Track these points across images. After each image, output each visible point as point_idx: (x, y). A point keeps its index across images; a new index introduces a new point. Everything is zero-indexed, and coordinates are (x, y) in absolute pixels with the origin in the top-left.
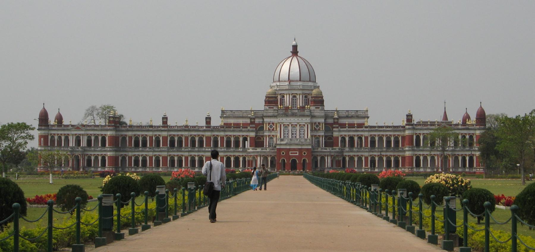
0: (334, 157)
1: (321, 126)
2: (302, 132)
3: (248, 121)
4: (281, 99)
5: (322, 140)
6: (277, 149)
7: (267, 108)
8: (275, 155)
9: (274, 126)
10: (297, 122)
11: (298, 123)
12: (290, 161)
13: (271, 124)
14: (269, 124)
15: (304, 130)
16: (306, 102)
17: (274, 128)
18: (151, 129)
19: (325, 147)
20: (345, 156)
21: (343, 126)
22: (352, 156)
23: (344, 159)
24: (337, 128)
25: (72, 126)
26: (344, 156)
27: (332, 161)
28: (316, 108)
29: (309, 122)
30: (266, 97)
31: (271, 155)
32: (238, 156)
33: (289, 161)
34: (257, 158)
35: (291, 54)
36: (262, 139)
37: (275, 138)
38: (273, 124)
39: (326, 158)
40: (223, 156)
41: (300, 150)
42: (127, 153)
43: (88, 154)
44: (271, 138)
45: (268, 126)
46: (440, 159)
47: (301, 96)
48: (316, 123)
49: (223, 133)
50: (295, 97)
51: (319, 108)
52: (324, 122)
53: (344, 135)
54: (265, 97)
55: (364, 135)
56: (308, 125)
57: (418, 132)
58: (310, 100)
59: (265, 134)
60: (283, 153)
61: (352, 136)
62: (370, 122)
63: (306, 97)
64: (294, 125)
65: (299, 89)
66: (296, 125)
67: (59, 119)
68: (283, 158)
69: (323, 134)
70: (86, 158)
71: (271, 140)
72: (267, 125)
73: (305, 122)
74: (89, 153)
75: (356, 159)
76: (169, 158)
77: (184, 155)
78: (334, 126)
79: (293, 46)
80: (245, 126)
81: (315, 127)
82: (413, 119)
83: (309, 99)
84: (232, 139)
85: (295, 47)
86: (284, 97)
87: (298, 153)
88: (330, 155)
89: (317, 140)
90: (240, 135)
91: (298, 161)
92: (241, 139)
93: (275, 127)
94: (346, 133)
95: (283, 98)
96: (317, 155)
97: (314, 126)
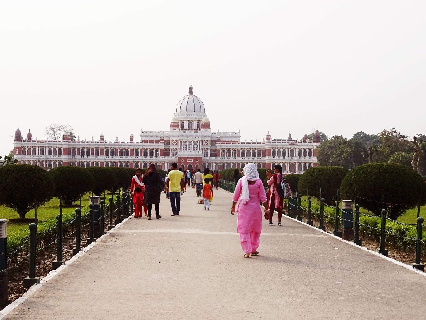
0: (217, 164)
1: (208, 143)
2: (196, 146)
3: (159, 139)
4: (181, 124)
5: (209, 152)
6: (179, 157)
7: (171, 129)
8: (177, 162)
14: (173, 140)
15: (196, 145)
16: (199, 126)
17: (176, 143)
18: (93, 143)
19: (211, 156)
20: (225, 163)
21: (223, 142)
22: (229, 163)
23: (224, 164)
24: (219, 143)
25: (38, 141)
26: (224, 163)
27: (216, 166)
28: (205, 130)
29: (201, 139)
30: (171, 123)
34: (165, 164)
35: (188, 94)
36: (168, 151)
37: (177, 150)
38: (176, 140)
39: (212, 164)
41: (195, 159)
42: (76, 160)
43: (49, 161)
44: (175, 150)
46: (289, 165)
47: (195, 122)
48: (205, 140)
50: (191, 122)
52: (210, 140)
56: (199, 142)
57: (274, 147)
58: (201, 125)
59: (170, 148)
60: (183, 161)
62: (242, 140)
63: (198, 122)
64: (190, 142)
65: (194, 118)
66: (192, 142)
67: (29, 137)
68: (183, 164)
69: (210, 148)
70: (48, 163)
71: (175, 152)
72: (172, 141)
74: (50, 160)
76: (105, 164)
77: (115, 161)
78: (217, 142)
79: (190, 88)
80: (157, 141)
81: (205, 143)
82: (271, 138)
83: (200, 124)
84: (148, 151)
85: (191, 89)
86: (183, 122)
87: (193, 161)
88: (214, 162)
89: (205, 152)
92: (154, 151)
94: (226, 146)
95: (183, 123)
96: (206, 162)
97: (203, 142)
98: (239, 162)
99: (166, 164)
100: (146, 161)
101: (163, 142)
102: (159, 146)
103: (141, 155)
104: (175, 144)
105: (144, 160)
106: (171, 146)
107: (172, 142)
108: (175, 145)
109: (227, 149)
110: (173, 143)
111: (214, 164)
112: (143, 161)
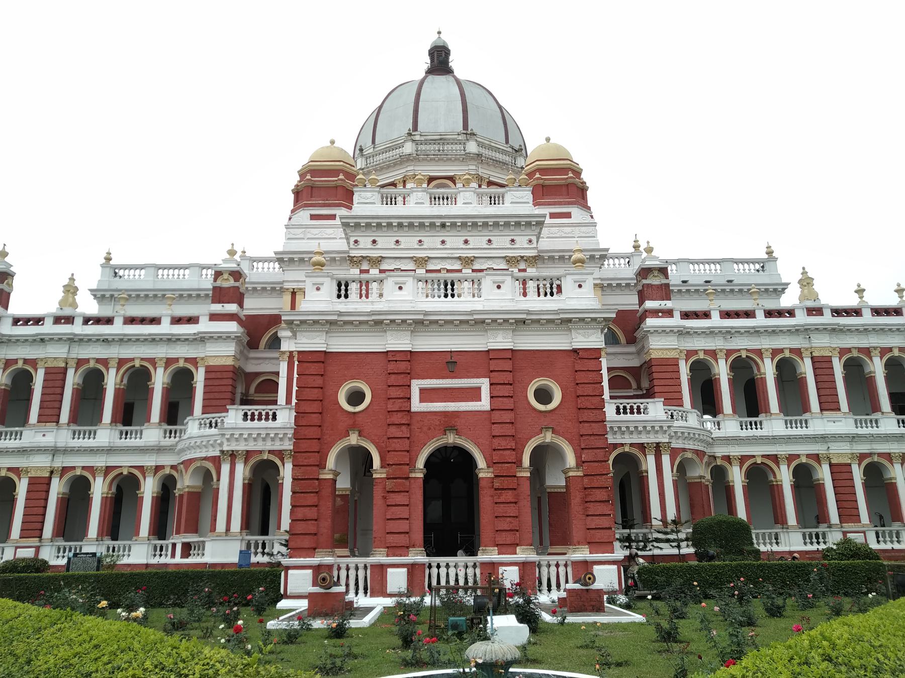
7: (304, 216)
10: (459, 258)
11: (467, 261)
12: (420, 463)
23: (719, 473)
26: (719, 462)
30: (302, 175)
32: (136, 472)
39: (649, 464)
40: (47, 475)
49: (65, 350)
51: (568, 215)
53: (706, 352)
54: (298, 179)
55: (807, 349)
60: (356, 397)
61: (744, 354)
68: (353, 439)
73: (510, 253)
75: (785, 476)
90: (153, 361)
91: (491, 464)
98: (840, 451)
100: (79, 461)
101: (232, 308)
102: (201, 339)
103: (49, 415)
105: (67, 451)
109: (729, 353)
111: (666, 459)
112: (60, 462)
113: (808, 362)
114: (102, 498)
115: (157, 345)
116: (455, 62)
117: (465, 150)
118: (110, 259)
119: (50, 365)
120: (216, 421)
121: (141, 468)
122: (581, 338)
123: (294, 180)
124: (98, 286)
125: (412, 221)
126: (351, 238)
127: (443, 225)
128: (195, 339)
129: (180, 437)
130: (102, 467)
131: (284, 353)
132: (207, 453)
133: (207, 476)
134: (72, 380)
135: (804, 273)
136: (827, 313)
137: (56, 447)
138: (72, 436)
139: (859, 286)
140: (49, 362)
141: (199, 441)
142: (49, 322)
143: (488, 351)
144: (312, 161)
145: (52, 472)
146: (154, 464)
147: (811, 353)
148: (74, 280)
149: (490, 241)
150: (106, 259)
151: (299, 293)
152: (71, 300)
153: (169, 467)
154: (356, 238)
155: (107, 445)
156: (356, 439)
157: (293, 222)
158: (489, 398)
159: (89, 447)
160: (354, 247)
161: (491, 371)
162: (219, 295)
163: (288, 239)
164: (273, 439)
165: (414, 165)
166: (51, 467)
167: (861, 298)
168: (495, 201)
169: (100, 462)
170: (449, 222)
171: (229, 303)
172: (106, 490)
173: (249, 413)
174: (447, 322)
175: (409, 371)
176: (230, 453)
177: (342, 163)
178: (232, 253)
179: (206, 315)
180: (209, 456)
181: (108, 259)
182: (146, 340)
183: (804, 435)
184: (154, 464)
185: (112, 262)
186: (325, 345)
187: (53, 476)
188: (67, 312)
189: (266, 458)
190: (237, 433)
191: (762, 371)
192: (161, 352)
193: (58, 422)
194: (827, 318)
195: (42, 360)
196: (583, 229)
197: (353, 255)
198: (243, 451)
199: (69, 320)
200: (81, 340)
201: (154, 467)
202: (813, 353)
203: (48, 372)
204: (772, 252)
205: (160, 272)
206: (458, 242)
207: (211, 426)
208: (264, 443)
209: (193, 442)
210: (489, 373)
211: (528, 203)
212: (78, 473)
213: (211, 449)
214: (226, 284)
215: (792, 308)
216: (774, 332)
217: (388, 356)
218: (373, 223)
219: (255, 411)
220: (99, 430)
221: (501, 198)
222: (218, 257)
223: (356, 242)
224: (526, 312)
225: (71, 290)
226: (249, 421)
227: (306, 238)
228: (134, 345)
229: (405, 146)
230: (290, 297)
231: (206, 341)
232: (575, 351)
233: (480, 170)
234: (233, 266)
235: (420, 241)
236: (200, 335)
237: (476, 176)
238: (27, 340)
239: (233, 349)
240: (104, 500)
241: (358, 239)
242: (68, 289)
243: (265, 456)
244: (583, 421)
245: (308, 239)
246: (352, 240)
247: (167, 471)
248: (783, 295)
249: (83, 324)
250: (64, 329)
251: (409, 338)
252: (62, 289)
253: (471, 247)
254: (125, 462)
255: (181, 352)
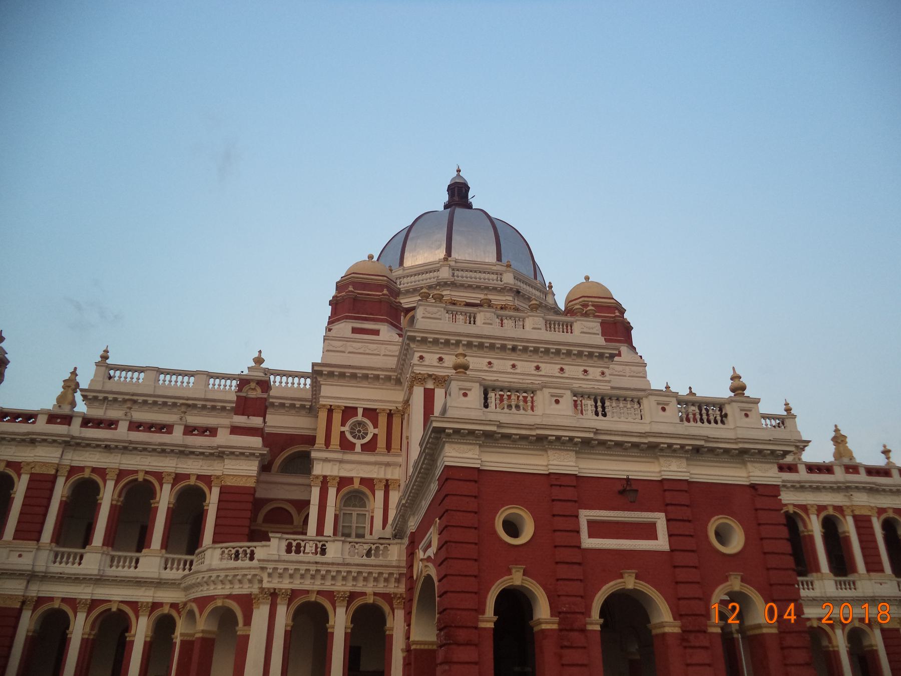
7: (345, 328)
9: (376, 426)
13: (360, 417)
14: (349, 412)
17: (375, 436)
31: (353, 596)
32: (127, 609)
33: (587, 612)
34: (248, 622)
37: (380, 494)
38: (371, 414)
40: (18, 606)
45: (343, 424)
49: (58, 454)
55: (848, 507)
60: (512, 528)
71: (355, 512)
72: (337, 417)
90: (159, 476)
93: (381, 431)
99: (261, 614)
101: (256, 421)
102: (220, 454)
104: (358, 443)
105: (46, 577)
106: (326, 460)
107: (337, 428)
108: (358, 448)
110: (349, 436)
112: (36, 590)
113: (850, 521)
114: (83, 639)
115: (166, 457)
116: (477, 199)
117: (501, 281)
118: (107, 358)
119: (37, 470)
120: (237, 552)
121: (134, 605)
122: (758, 473)
123: (332, 292)
124: (90, 385)
125: (483, 340)
126: (416, 353)
127: (514, 349)
128: (212, 454)
129: (190, 569)
130: (86, 600)
131: (317, 477)
132: (231, 590)
133: (225, 618)
134: (60, 491)
135: (837, 430)
136: (862, 471)
137: (35, 572)
138: (53, 559)
139: (885, 446)
140: (37, 468)
141: (222, 574)
142: (42, 419)
143: (662, 481)
144: (354, 273)
145: (23, 603)
146: (150, 600)
147: (852, 511)
148: (77, 375)
149: (562, 370)
150: (102, 357)
151: (337, 411)
152: (70, 397)
153: (169, 606)
154: (420, 354)
155: (96, 572)
156: (520, 579)
157: (333, 333)
158: (667, 536)
159: (74, 574)
160: (418, 363)
161: (667, 505)
162: (244, 406)
163: (328, 351)
164: (323, 578)
165: (451, 290)
166: (24, 596)
167: (888, 458)
168: (563, 329)
169: (84, 592)
170: (521, 346)
171: (254, 416)
172: (88, 630)
173: (294, 544)
174: (619, 444)
175: (576, 499)
176: (272, 591)
177: (385, 278)
178: (259, 360)
179: (228, 428)
180: (234, 593)
181: (105, 357)
182: (154, 450)
183: (856, 597)
184: (151, 600)
185: (108, 361)
186: (479, 461)
187: (24, 607)
188: (66, 410)
189: (313, 599)
190: (281, 566)
191: (810, 527)
192: (168, 465)
193: (38, 540)
194: (863, 477)
195: (28, 464)
196: (634, 368)
197: (418, 372)
198: (286, 590)
199: (67, 419)
200: (78, 444)
201: (150, 605)
202: (855, 512)
203: (35, 479)
204: (791, 410)
205: (162, 377)
206: (529, 367)
207: (237, 557)
208: (312, 581)
209: (214, 575)
210: (664, 507)
211: (598, 334)
212: (56, 606)
213: (237, 586)
214: (252, 395)
215: (830, 464)
216: (817, 488)
217: (553, 480)
218: (441, 339)
219: (292, 541)
220: (88, 554)
221: (569, 327)
222: (242, 366)
223: (421, 358)
224: (704, 438)
225: (71, 385)
226: (293, 553)
227: (347, 352)
228: (138, 455)
229: (440, 270)
230: (325, 414)
231: (225, 456)
232: (753, 487)
233: (516, 302)
234: (259, 375)
235: (490, 363)
236: (219, 449)
237: (513, 307)
238: (13, 440)
239: (256, 468)
240: (84, 642)
241: (424, 355)
242: (68, 384)
243: (313, 598)
244: (772, 569)
245: (349, 353)
246: (417, 355)
247: (166, 610)
248: (803, 452)
249: (81, 426)
250: (59, 429)
251: (574, 459)
252: (62, 384)
253: (544, 374)
254: (116, 595)
255: (193, 467)
